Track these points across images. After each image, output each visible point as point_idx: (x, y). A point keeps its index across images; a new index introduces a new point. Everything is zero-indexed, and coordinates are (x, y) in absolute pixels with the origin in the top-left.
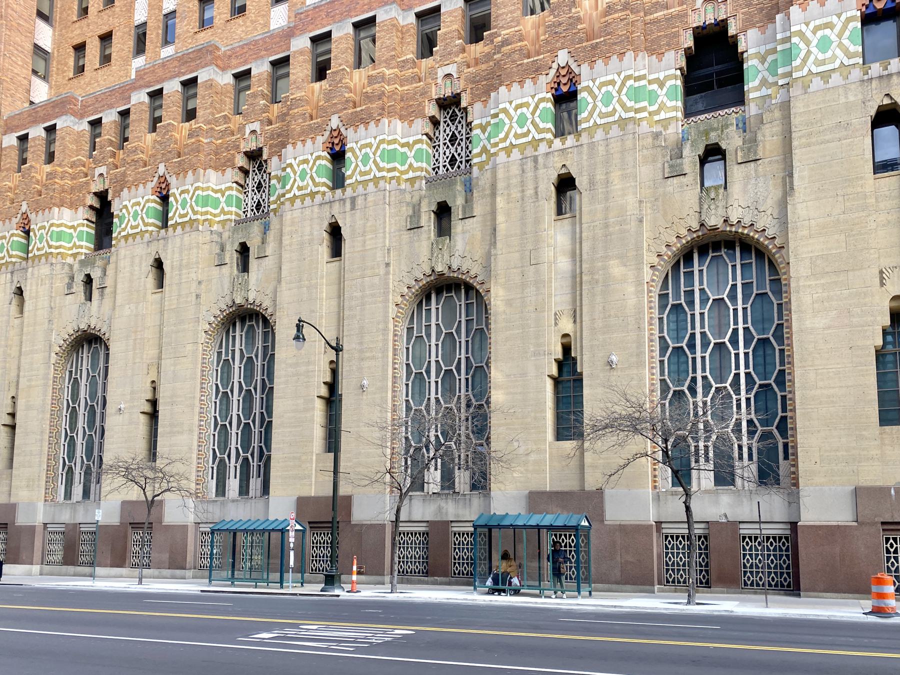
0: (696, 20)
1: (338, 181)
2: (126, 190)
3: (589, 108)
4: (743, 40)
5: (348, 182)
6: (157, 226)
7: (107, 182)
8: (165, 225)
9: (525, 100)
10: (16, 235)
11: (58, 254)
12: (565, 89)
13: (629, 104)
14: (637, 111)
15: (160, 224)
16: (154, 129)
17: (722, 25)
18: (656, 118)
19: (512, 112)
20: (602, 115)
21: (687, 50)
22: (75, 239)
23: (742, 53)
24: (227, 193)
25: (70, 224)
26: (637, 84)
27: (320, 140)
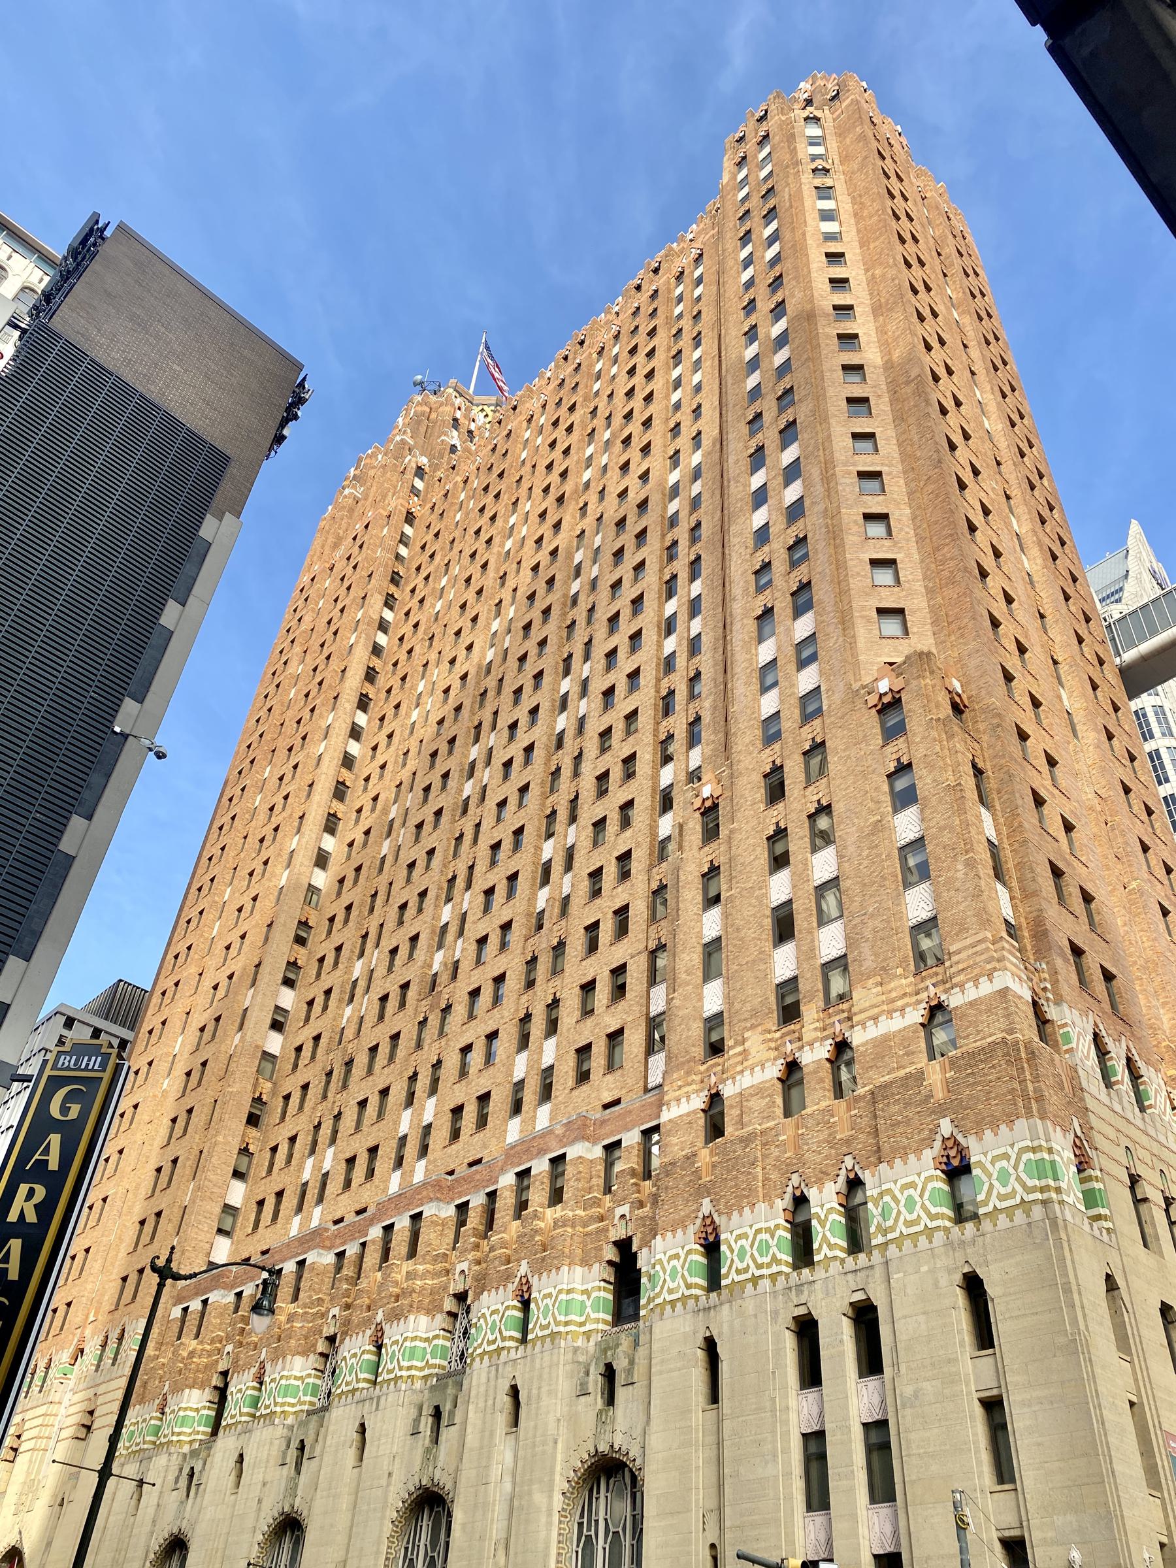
1: (714, 1281)
2: (486, 1293)
3: (990, 1186)
5: (724, 1283)
6: (517, 1340)
7: (469, 1281)
8: (524, 1340)
10: (369, 1352)
11: (409, 1377)
12: (955, 1163)
15: (518, 1335)
16: (518, 1216)
22: (428, 1356)
24: (594, 1295)
25: (425, 1336)
27: (692, 1229)
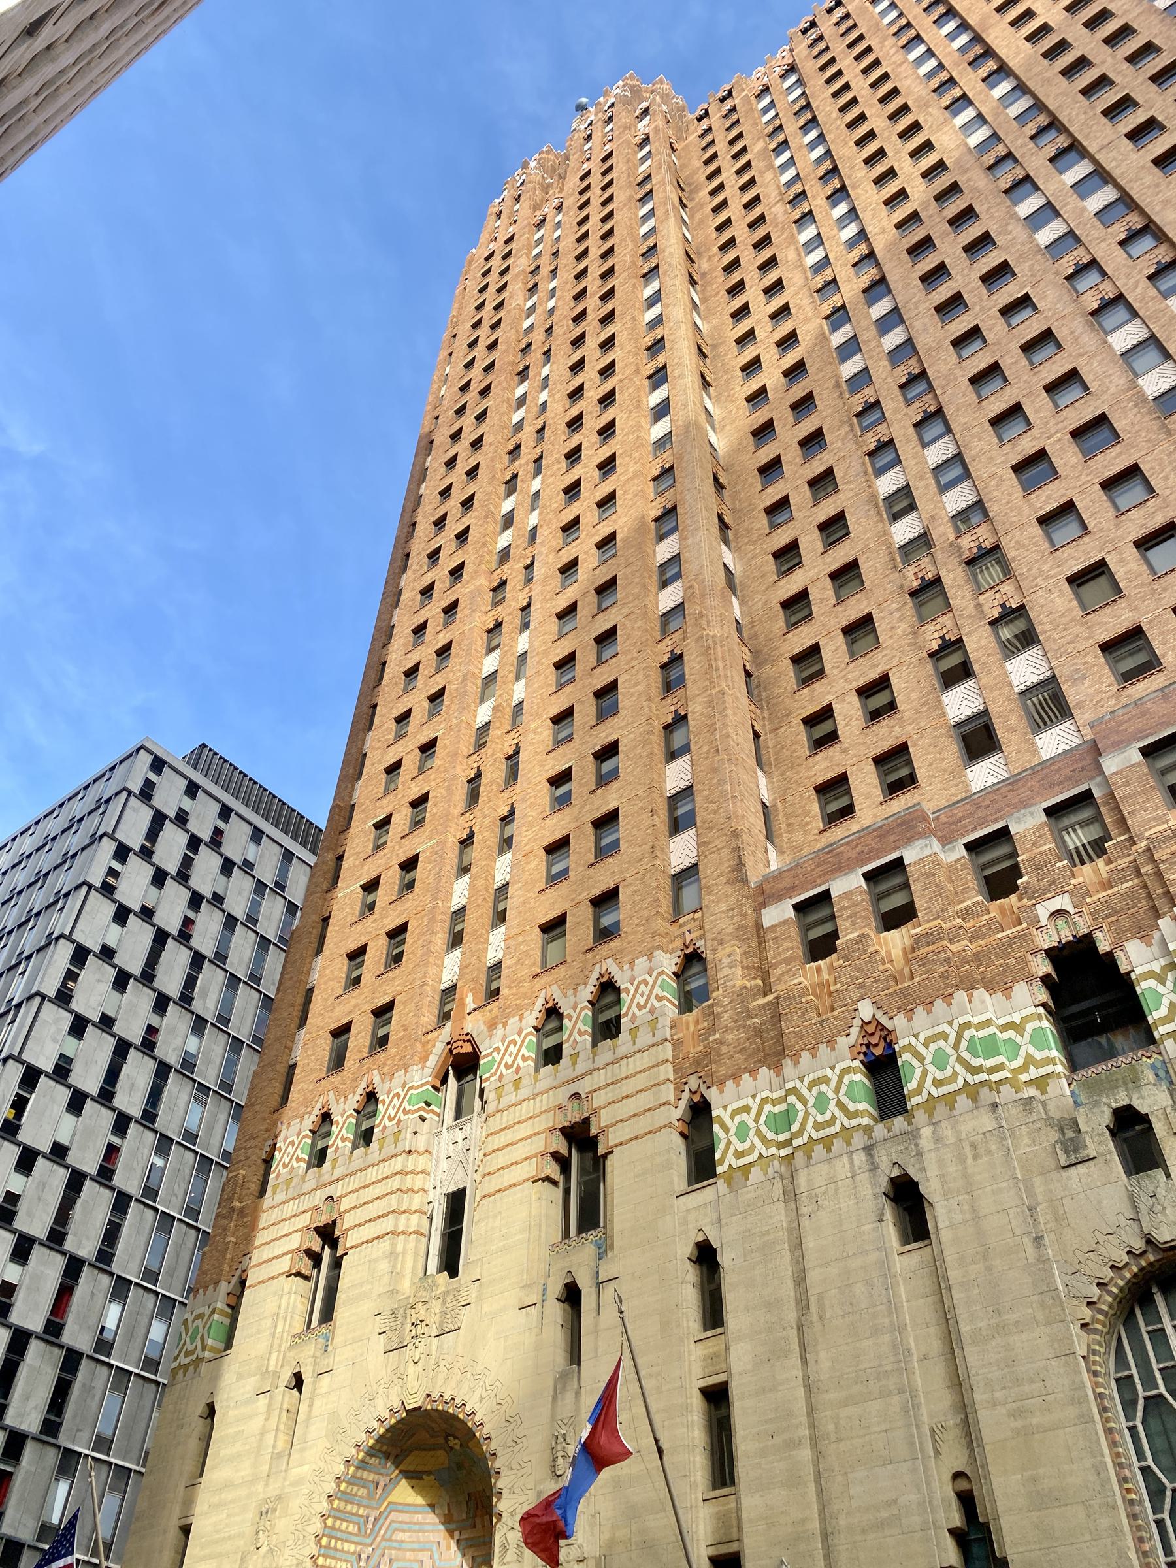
0: (1047, 940)
4: (1123, 958)
9: (820, 1074)
12: (878, 1051)
13: (975, 1062)
14: (992, 1070)
17: (1087, 942)
18: (1024, 1077)
19: (805, 1092)
20: (937, 1083)
21: (1046, 980)
23: (1128, 973)
26: (981, 1034)
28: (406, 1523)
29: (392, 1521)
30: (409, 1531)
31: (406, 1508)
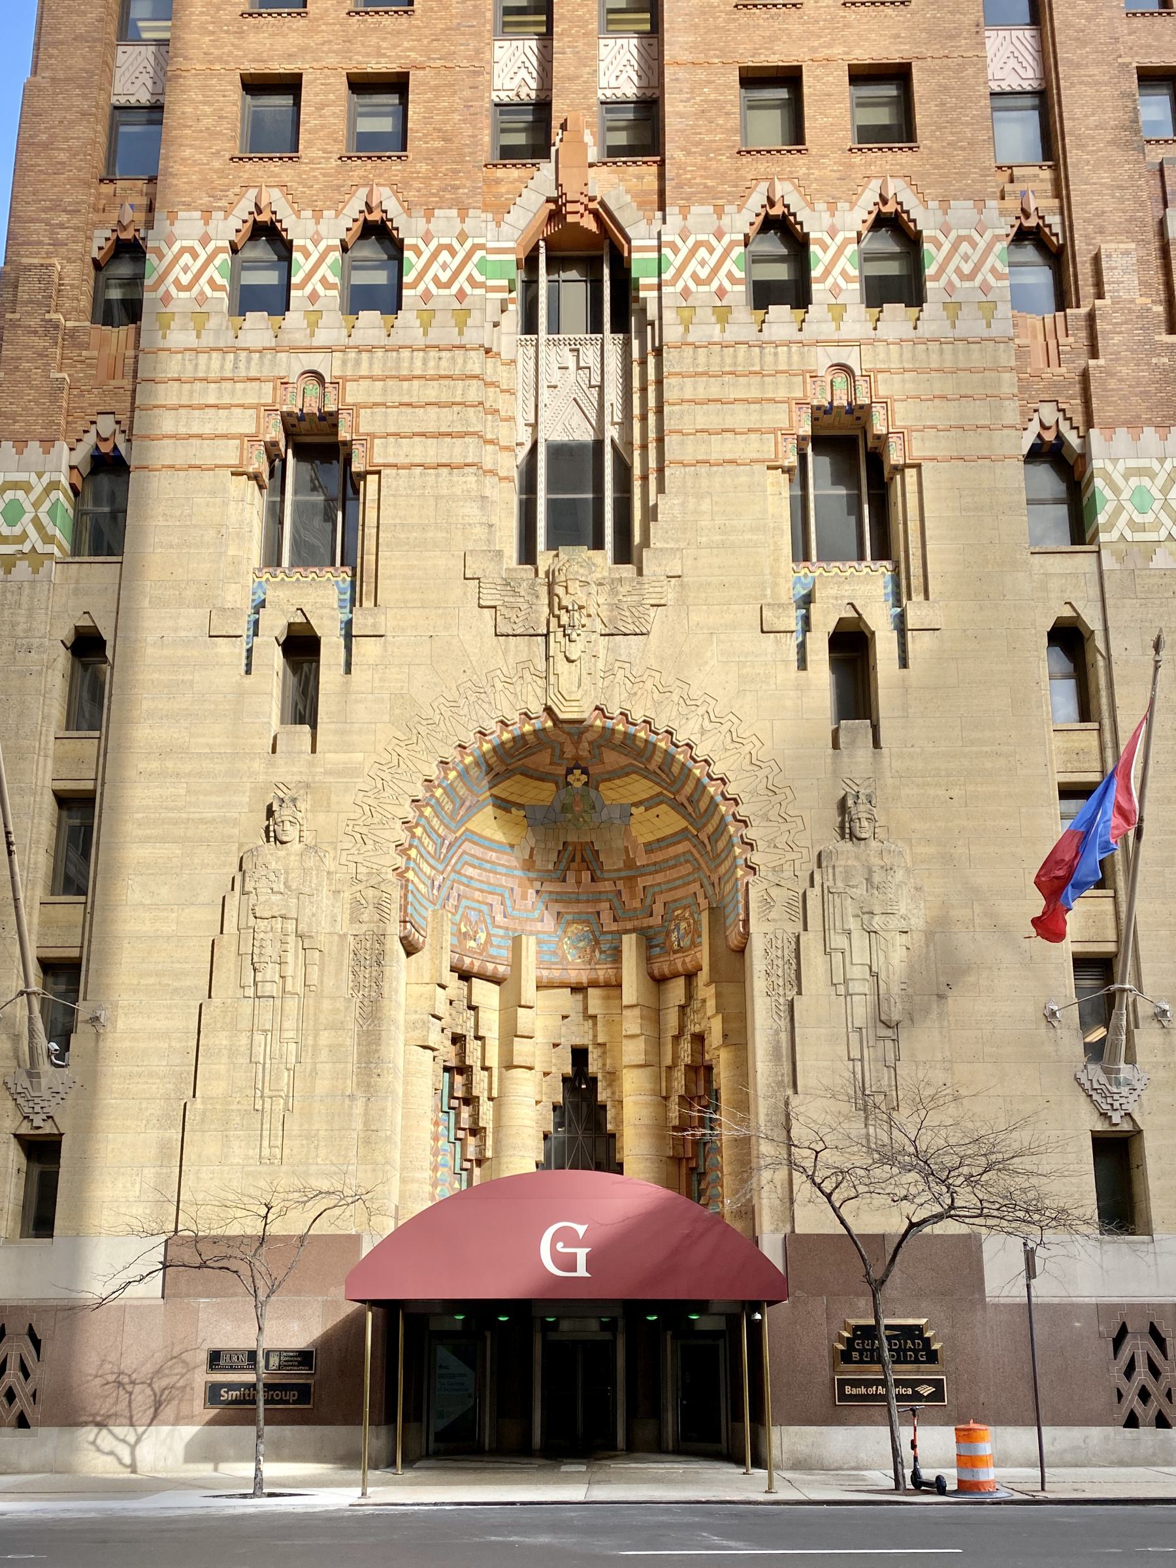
28: (478, 858)
29: (464, 852)
30: (480, 868)
31: (481, 841)
